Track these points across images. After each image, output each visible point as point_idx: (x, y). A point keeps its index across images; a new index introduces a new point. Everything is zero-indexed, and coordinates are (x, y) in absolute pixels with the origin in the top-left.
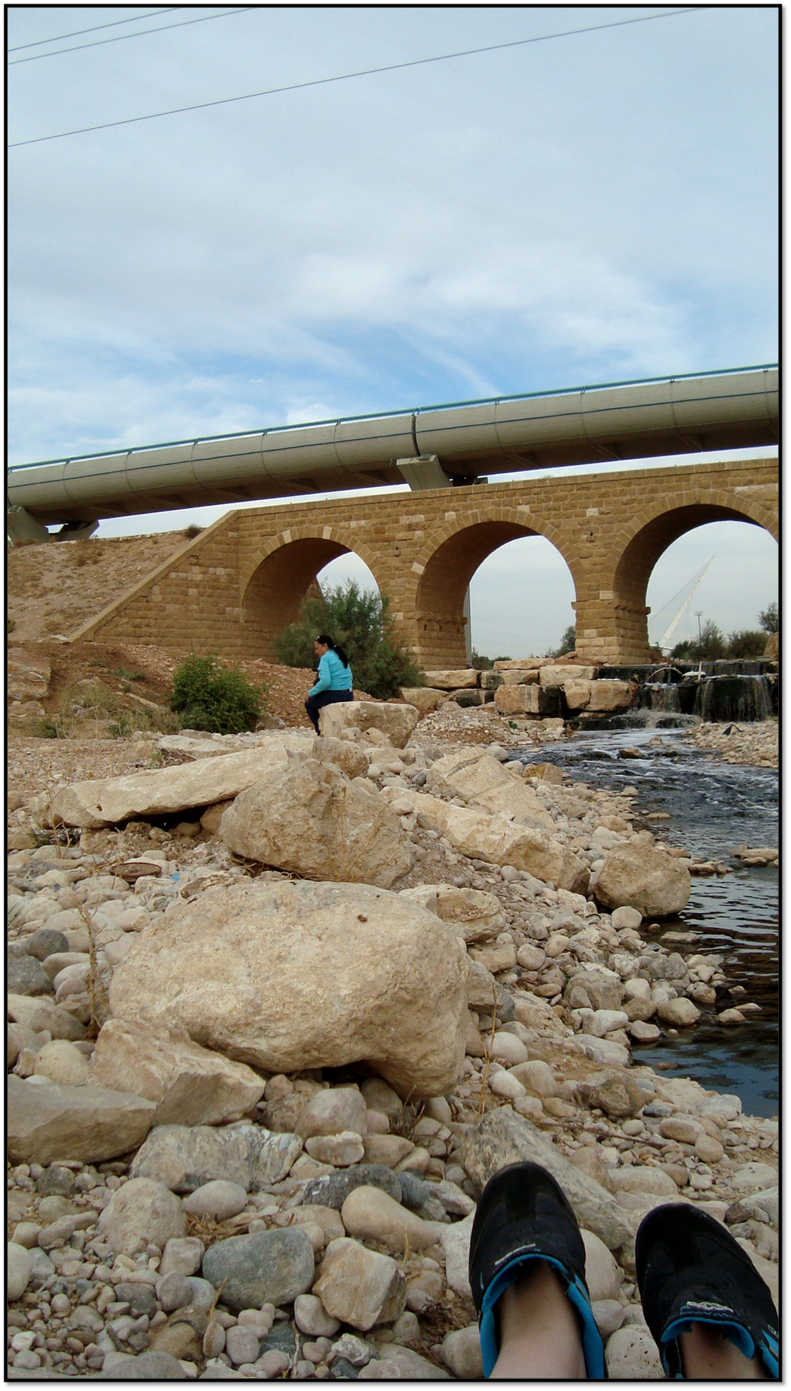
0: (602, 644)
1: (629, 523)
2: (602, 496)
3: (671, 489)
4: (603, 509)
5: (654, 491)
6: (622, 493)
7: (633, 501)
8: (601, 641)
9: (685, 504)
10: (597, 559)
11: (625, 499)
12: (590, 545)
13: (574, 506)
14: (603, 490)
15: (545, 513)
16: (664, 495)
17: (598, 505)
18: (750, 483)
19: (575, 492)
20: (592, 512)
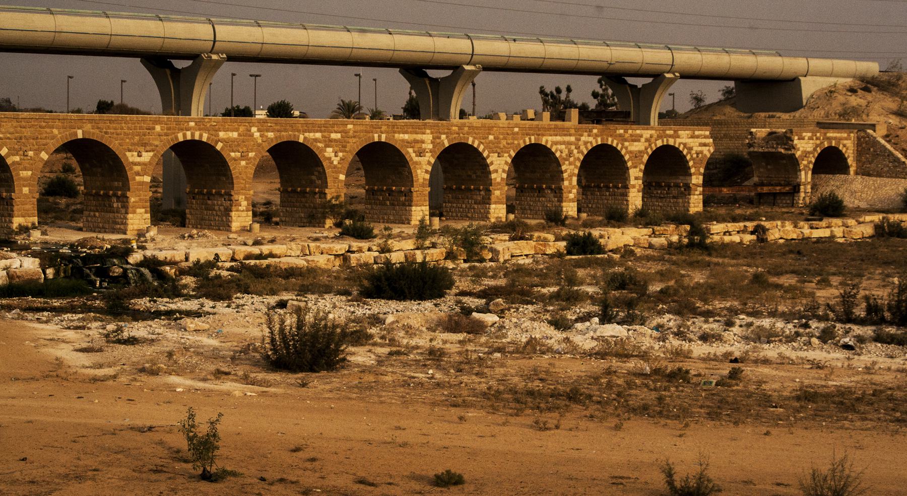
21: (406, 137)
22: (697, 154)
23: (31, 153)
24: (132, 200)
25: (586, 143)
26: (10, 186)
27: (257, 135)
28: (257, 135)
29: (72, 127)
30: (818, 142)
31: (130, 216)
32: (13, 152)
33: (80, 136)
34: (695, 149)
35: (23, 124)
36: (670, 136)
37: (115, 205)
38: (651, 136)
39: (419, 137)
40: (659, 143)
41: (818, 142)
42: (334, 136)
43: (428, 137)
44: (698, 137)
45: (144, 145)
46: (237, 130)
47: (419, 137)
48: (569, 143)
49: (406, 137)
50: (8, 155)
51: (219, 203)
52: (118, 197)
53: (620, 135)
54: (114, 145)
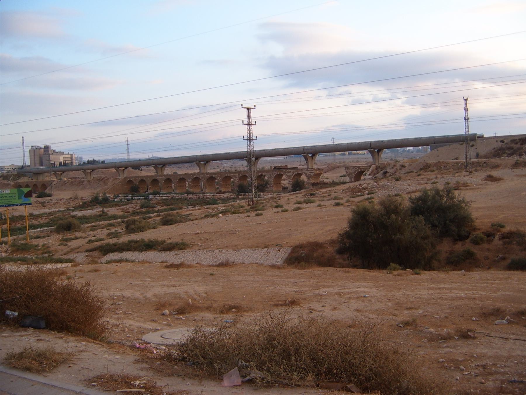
21: (233, 174)
22: (309, 175)
25: (275, 174)
27: (206, 176)
28: (206, 176)
30: (356, 170)
34: (308, 174)
36: (300, 171)
38: (294, 171)
39: (235, 174)
40: (296, 173)
41: (356, 170)
42: (219, 175)
44: (309, 171)
47: (235, 174)
48: (270, 174)
49: (233, 174)
53: (284, 172)
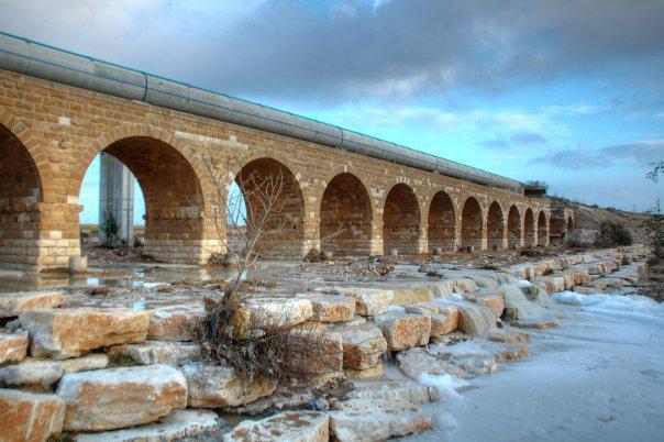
0: (67, 244)
1: (98, 139)
2: (75, 109)
3: (132, 119)
4: (76, 120)
5: (118, 117)
6: (93, 111)
7: (101, 121)
8: (66, 242)
9: (141, 134)
10: (67, 166)
11: (96, 117)
12: (61, 151)
13: (47, 110)
14: (76, 104)
15: (14, 108)
16: (127, 122)
17: (70, 115)
18: (185, 130)
19: (49, 97)
20: (64, 121)
23: (316, 181)
24: (374, 227)
26: (299, 211)
29: (341, 162)
31: (373, 241)
32: (305, 178)
33: (346, 171)
35: (312, 153)
37: (355, 233)
43: (486, 196)
45: (381, 183)
46: (420, 179)
50: (302, 180)
51: (405, 234)
52: (358, 226)
54: (364, 181)
